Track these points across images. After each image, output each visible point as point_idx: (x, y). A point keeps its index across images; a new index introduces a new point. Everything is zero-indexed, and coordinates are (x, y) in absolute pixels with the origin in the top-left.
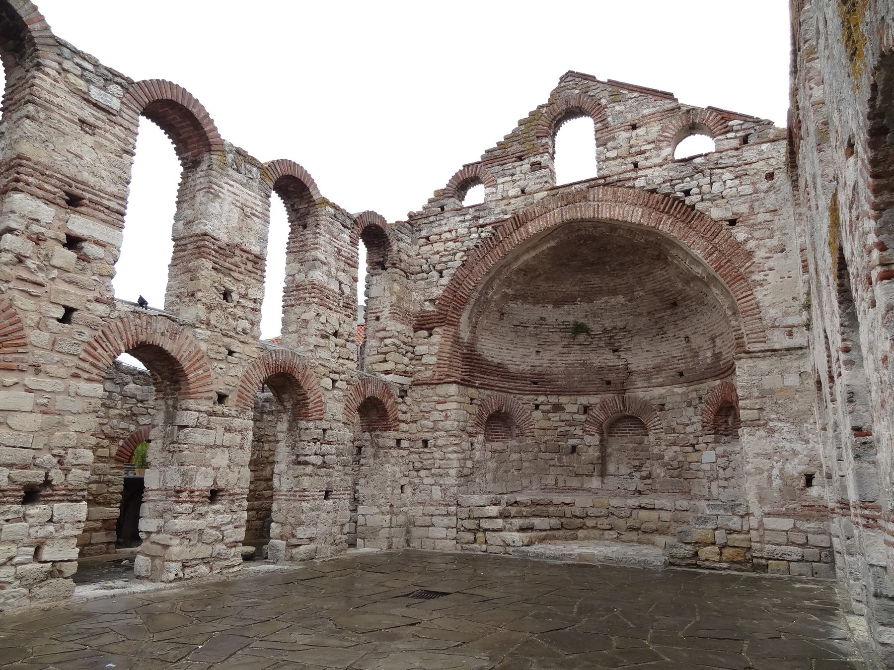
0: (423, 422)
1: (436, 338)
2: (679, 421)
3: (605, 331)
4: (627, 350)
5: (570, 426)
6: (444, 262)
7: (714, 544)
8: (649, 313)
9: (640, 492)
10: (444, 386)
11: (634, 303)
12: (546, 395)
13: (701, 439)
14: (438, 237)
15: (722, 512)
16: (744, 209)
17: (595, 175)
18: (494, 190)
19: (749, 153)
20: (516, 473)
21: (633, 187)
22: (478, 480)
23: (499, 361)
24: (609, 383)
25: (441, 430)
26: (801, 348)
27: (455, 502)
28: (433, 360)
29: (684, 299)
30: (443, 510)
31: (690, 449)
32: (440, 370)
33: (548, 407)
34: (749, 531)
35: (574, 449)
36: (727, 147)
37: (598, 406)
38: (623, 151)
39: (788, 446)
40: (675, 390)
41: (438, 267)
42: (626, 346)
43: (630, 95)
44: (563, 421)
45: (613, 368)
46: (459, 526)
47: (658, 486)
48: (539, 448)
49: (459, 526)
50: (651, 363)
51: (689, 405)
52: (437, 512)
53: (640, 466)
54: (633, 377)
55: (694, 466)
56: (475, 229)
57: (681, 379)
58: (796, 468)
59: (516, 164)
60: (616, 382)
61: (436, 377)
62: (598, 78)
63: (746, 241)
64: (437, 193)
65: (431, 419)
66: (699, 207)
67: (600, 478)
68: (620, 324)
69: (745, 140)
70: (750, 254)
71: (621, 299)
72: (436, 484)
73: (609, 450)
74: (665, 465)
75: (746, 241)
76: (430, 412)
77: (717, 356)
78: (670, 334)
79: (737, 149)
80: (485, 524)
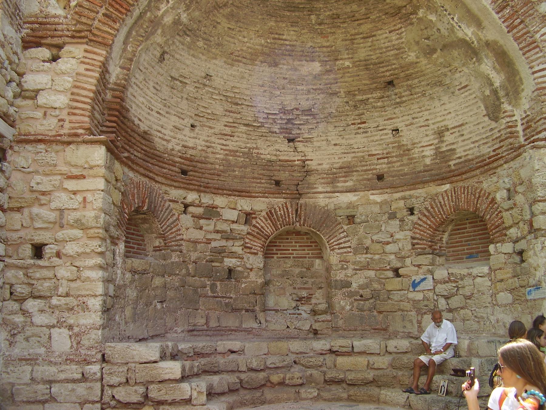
0: (36, 210)
2: (375, 238)
3: (284, 111)
4: (308, 140)
5: (227, 239)
8: (348, 93)
10: (83, 148)
11: (332, 76)
12: (199, 191)
13: (408, 261)
20: (159, 306)
22: (117, 318)
23: (146, 129)
24: (278, 183)
25: (72, 227)
27: (99, 356)
28: (61, 100)
29: (408, 77)
30: (74, 371)
31: (390, 274)
32: (73, 118)
33: (200, 211)
35: (230, 271)
37: (264, 213)
40: (372, 197)
42: (306, 136)
44: (218, 232)
45: (286, 165)
46: (106, 399)
47: (340, 323)
48: (188, 269)
49: (106, 399)
50: (338, 162)
51: (392, 216)
52: (62, 376)
53: (309, 298)
54: (312, 179)
55: (396, 296)
57: (380, 184)
60: (290, 182)
61: (65, 131)
65: (53, 205)
68: (305, 104)
71: (316, 67)
72: (60, 324)
74: (351, 295)
78: (371, 124)
80: (155, 393)
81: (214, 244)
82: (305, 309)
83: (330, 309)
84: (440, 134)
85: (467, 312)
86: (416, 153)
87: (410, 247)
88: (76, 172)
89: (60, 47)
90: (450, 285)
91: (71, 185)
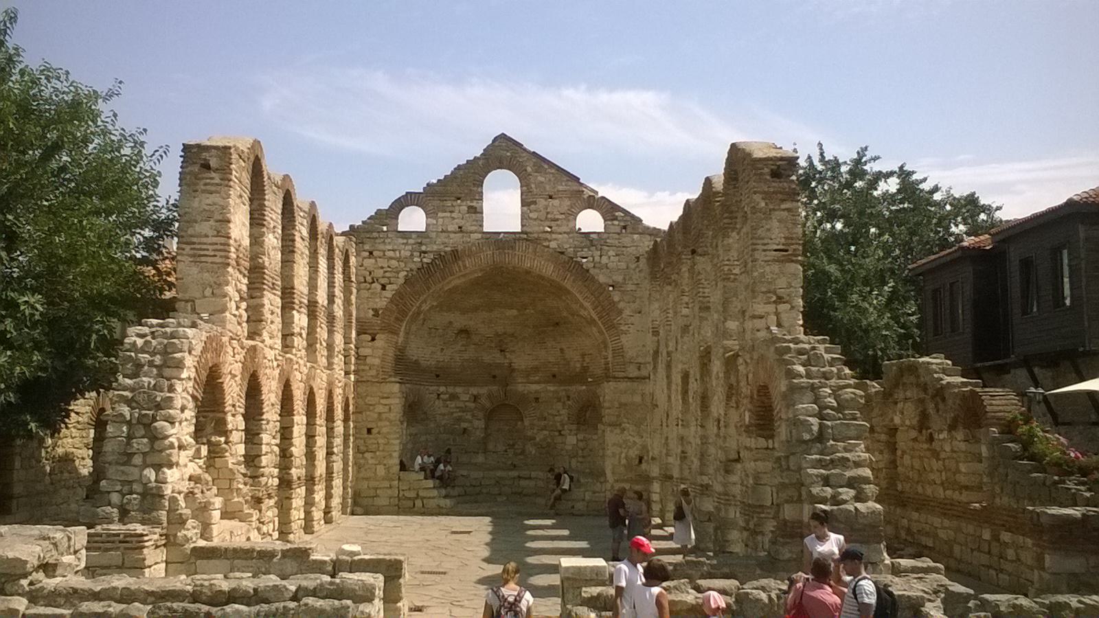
0: (368, 413)
1: (381, 341)
2: (550, 412)
3: (497, 335)
5: (463, 412)
6: (389, 278)
7: (583, 500)
9: (515, 466)
13: (566, 426)
14: (382, 254)
15: (590, 480)
16: (619, 278)
17: (520, 230)
18: (435, 222)
19: (626, 240)
21: (548, 247)
24: (494, 377)
26: (644, 378)
28: (377, 361)
29: (565, 323)
31: (557, 434)
34: (605, 492)
35: (465, 429)
36: (612, 231)
38: (542, 215)
39: (632, 439)
40: (548, 388)
41: (383, 281)
43: (549, 170)
51: (559, 400)
52: (383, 486)
53: (513, 445)
54: (515, 374)
56: (418, 254)
58: (634, 453)
59: (454, 204)
60: (502, 376)
62: (525, 146)
63: (619, 301)
64: (379, 212)
65: (376, 410)
66: (590, 271)
67: (483, 455)
69: (625, 227)
70: (620, 312)
71: (515, 312)
72: (379, 464)
73: (489, 431)
74: (535, 445)
75: (619, 301)
76: (374, 405)
77: (585, 369)
79: (619, 234)
80: (422, 494)
81: (455, 415)
82: (511, 453)
83: (523, 452)
84: (583, 355)
85: (589, 459)
86: (572, 364)
87: (566, 419)
88: (385, 395)
89: (376, 335)
90: (584, 443)
91: (383, 401)
